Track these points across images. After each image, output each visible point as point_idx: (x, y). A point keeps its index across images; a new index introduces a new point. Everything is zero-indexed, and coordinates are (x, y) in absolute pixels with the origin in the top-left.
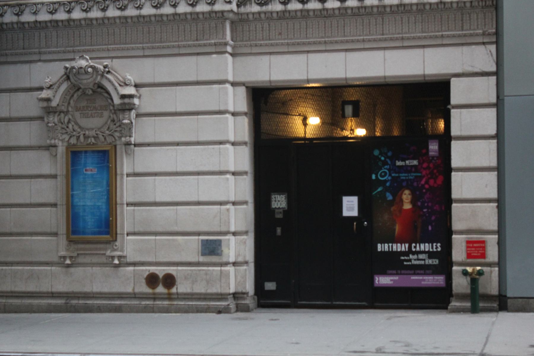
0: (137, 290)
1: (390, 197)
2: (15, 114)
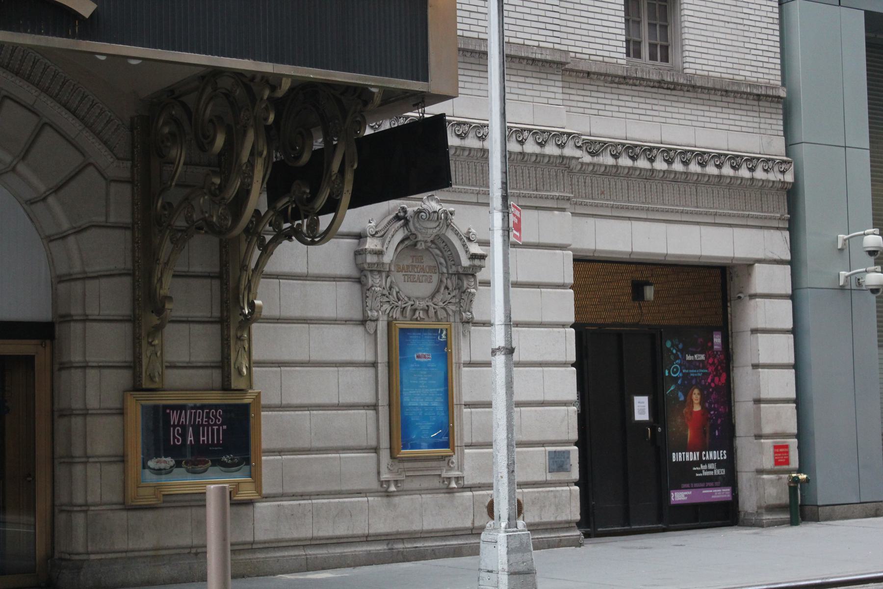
1: (682, 398)
2: (314, 270)
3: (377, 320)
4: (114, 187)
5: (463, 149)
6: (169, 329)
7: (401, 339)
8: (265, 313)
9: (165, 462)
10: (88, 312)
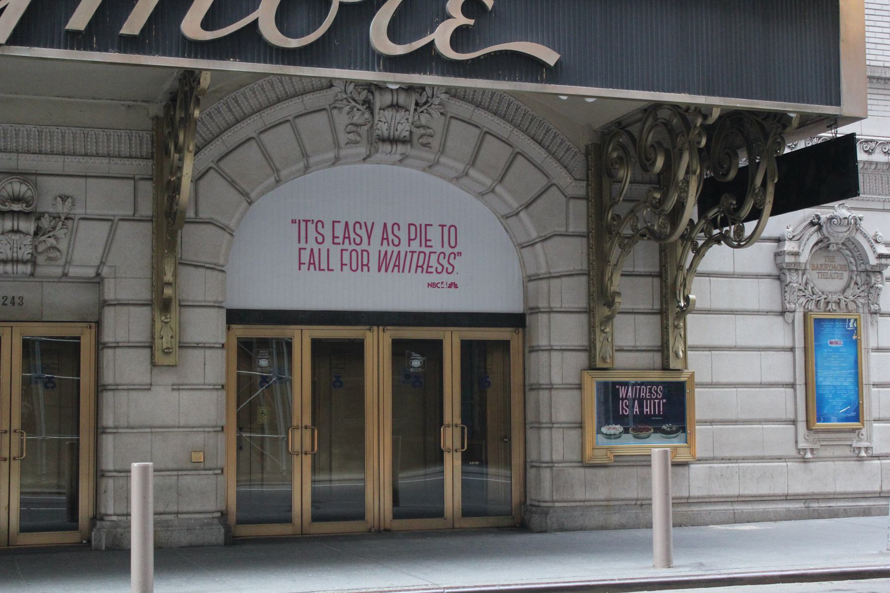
0: (884, 489)
2: (739, 270)
3: (794, 311)
4: (572, 202)
5: (871, 163)
6: (618, 319)
7: (816, 327)
8: (698, 305)
9: (614, 428)
10: (553, 305)
